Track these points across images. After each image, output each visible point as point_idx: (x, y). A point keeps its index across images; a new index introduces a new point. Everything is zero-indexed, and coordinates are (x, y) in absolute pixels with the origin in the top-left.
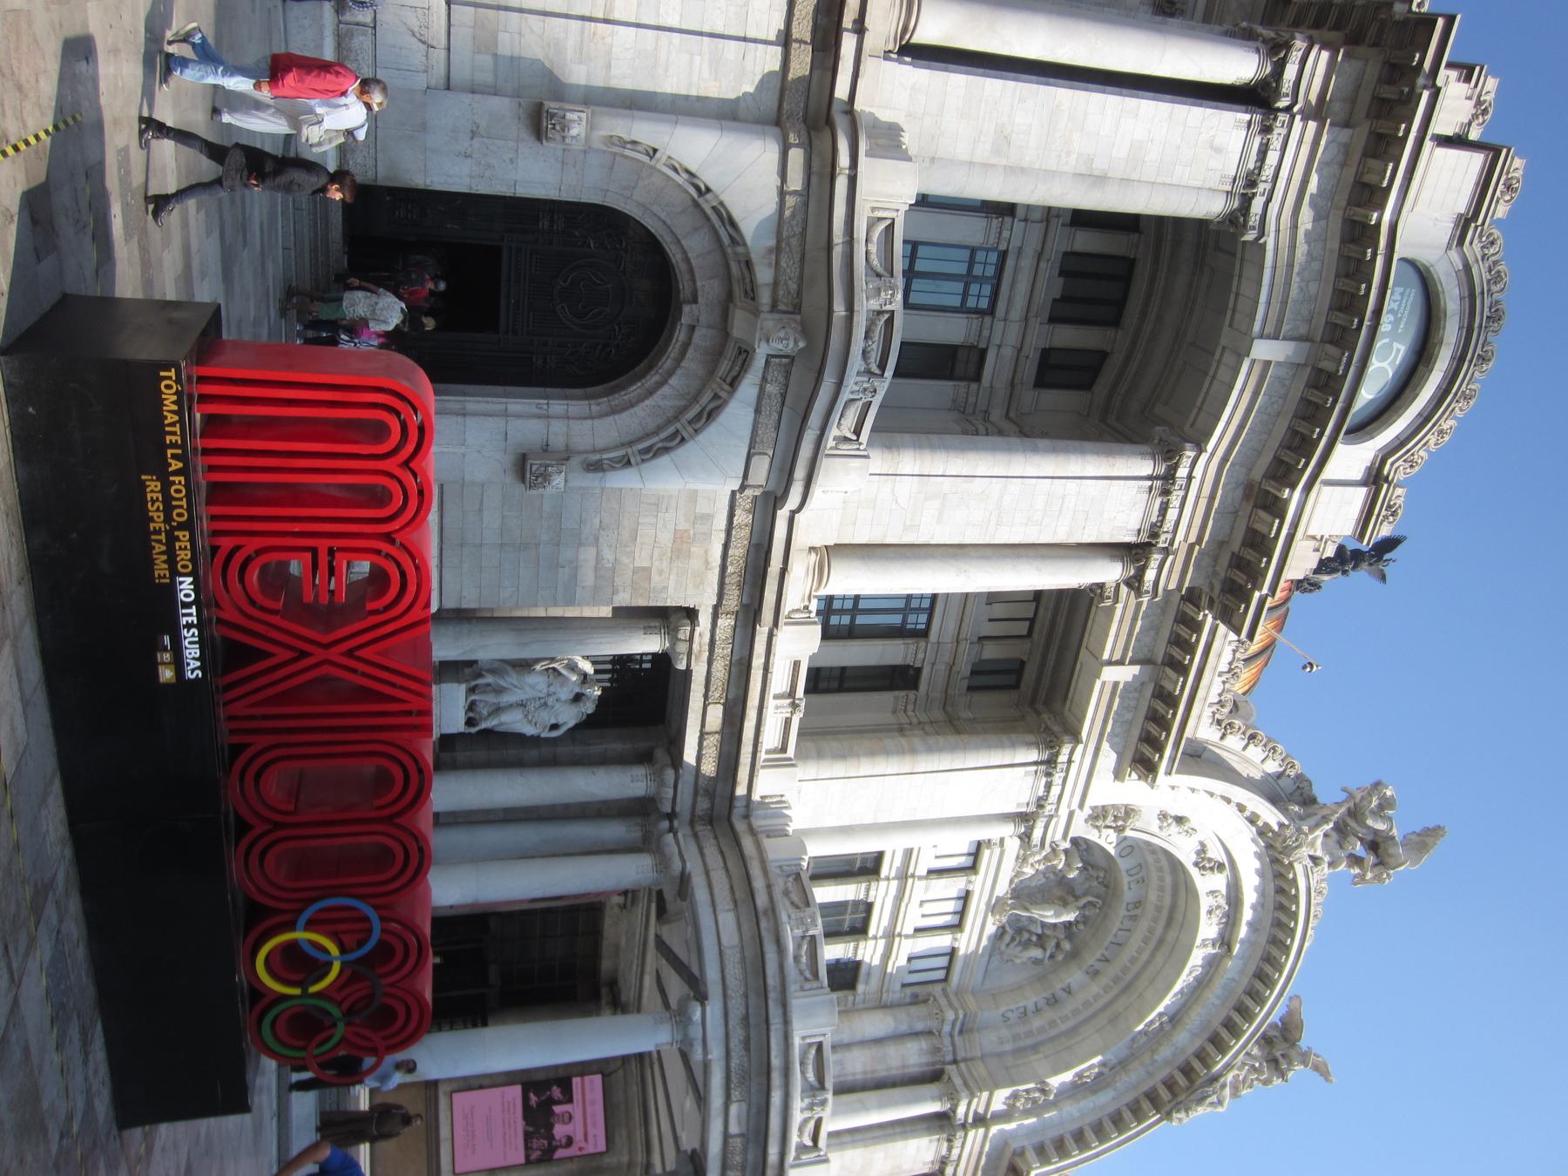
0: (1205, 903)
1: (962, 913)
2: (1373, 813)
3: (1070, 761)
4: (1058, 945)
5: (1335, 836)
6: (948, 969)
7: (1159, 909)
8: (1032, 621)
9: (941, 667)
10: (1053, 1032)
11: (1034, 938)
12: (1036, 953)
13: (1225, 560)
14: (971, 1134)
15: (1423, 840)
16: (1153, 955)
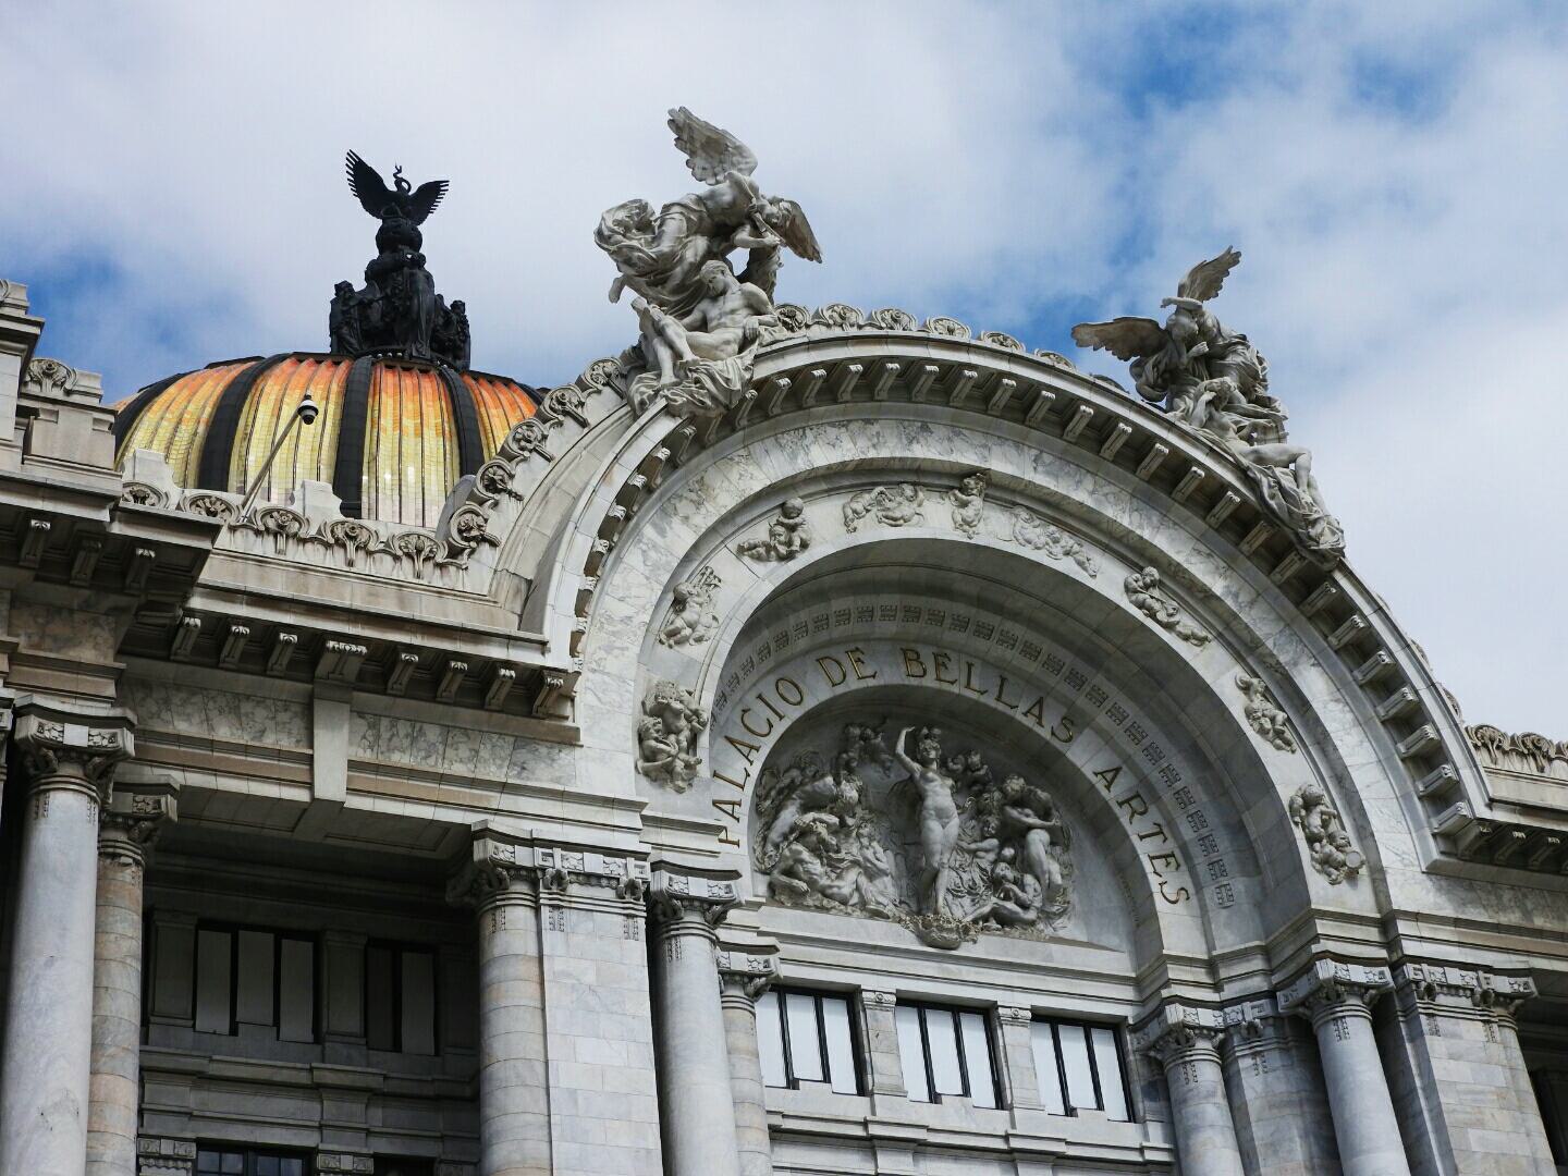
0: (872, 531)
1: (957, 1009)
2: (657, 239)
3: (532, 843)
4: (1020, 802)
5: (704, 305)
6: (1088, 1024)
7: (913, 614)
8: (281, 934)
9: (377, 1117)
10: (1200, 795)
11: (1009, 852)
12: (1038, 840)
13: (56, 593)
14: (1410, 948)
15: (700, 142)
16: (1015, 616)
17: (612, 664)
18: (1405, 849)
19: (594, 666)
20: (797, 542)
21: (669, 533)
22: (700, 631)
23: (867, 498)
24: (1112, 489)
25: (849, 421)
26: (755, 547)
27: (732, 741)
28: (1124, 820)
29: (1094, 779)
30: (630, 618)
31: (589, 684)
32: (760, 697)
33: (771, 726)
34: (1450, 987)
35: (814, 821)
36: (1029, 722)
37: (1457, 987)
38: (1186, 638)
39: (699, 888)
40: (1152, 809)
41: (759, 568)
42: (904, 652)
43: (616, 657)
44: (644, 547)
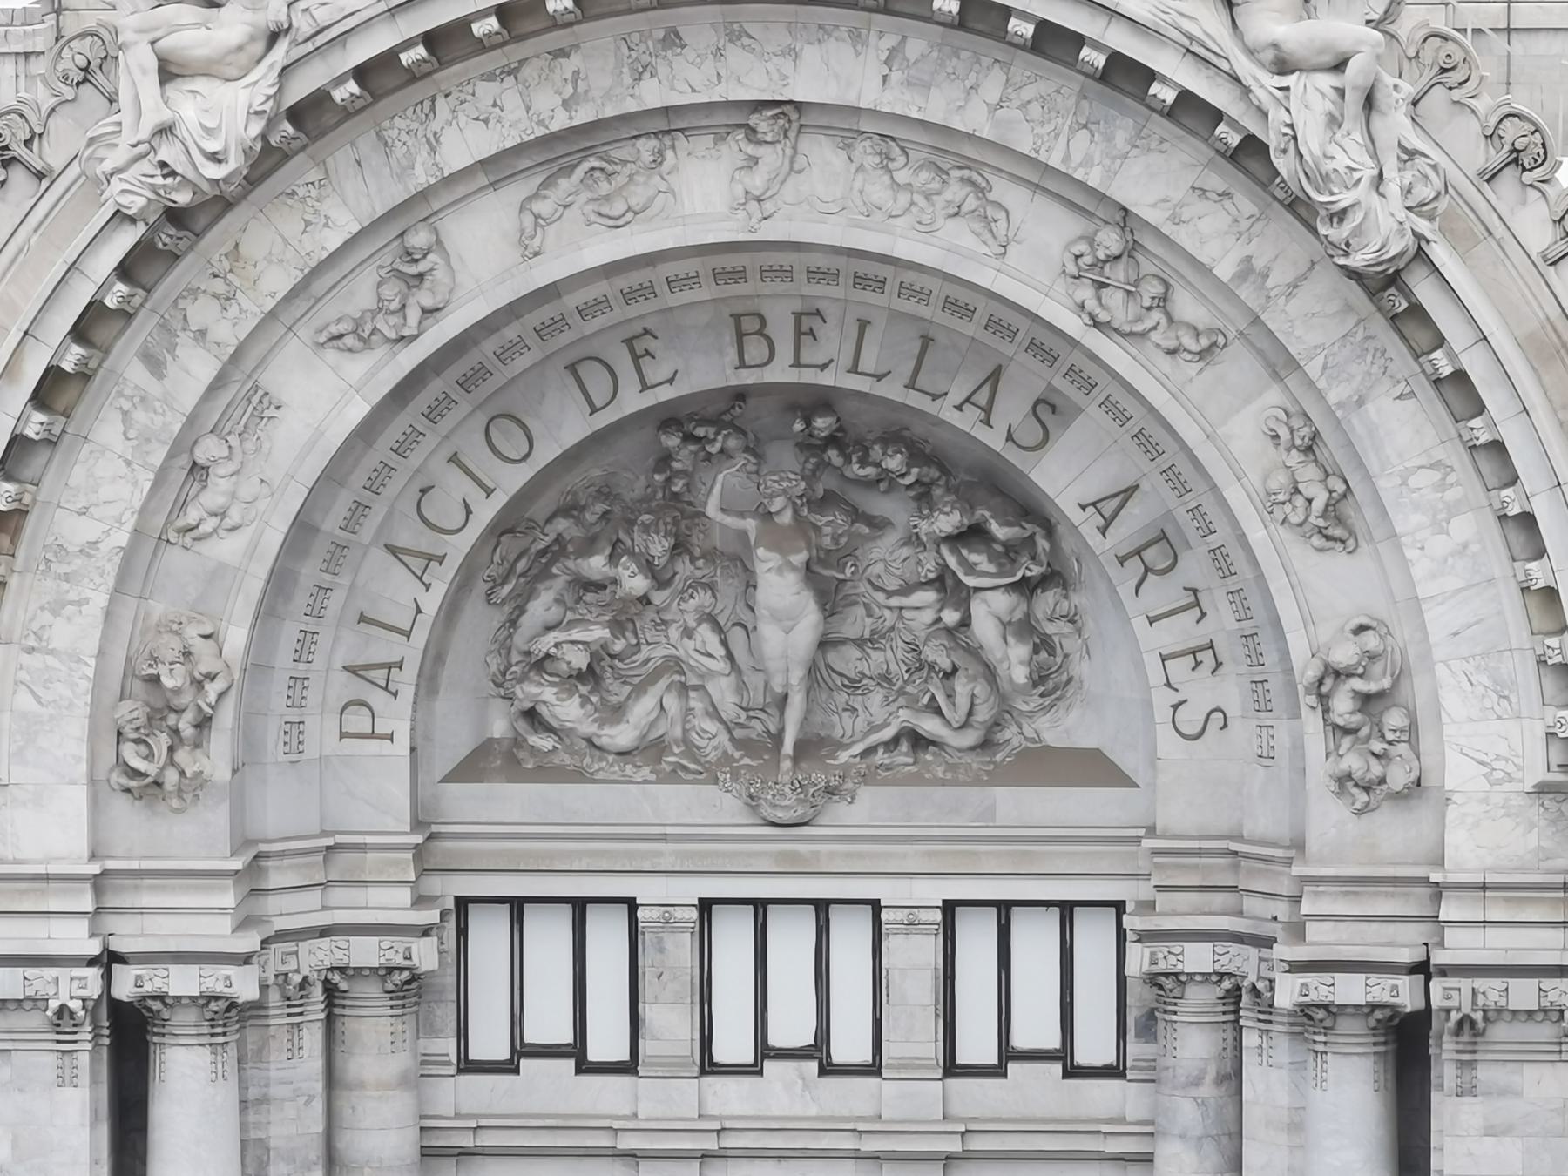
4: (973, 535)
11: (951, 617)
12: (990, 612)
17: (62, 634)
18: (1502, 750)
19: (32, 642)
20: (413, 315)
21: (172, 369)
22: (234, 516)
23: (564, 184)
24: (1043, 87)
25: (522, 62)
26: (341, 336)
27: (393, 550)
28: (1125, 591)
29: (1075, 515)
30: (94, 544)
31: (23, 675)
32: (454, 459)
33: (469, 512)
34: (1514, 1012)
35: (556, 645)
36: (967, 421)
37: (1530, 1013)
38: (1172, 352)
39: (182, 982)
40: (1185, 560)
41: (357, 367)
42: (737, 318)
43: (69, 619)
44: (127, 405)
